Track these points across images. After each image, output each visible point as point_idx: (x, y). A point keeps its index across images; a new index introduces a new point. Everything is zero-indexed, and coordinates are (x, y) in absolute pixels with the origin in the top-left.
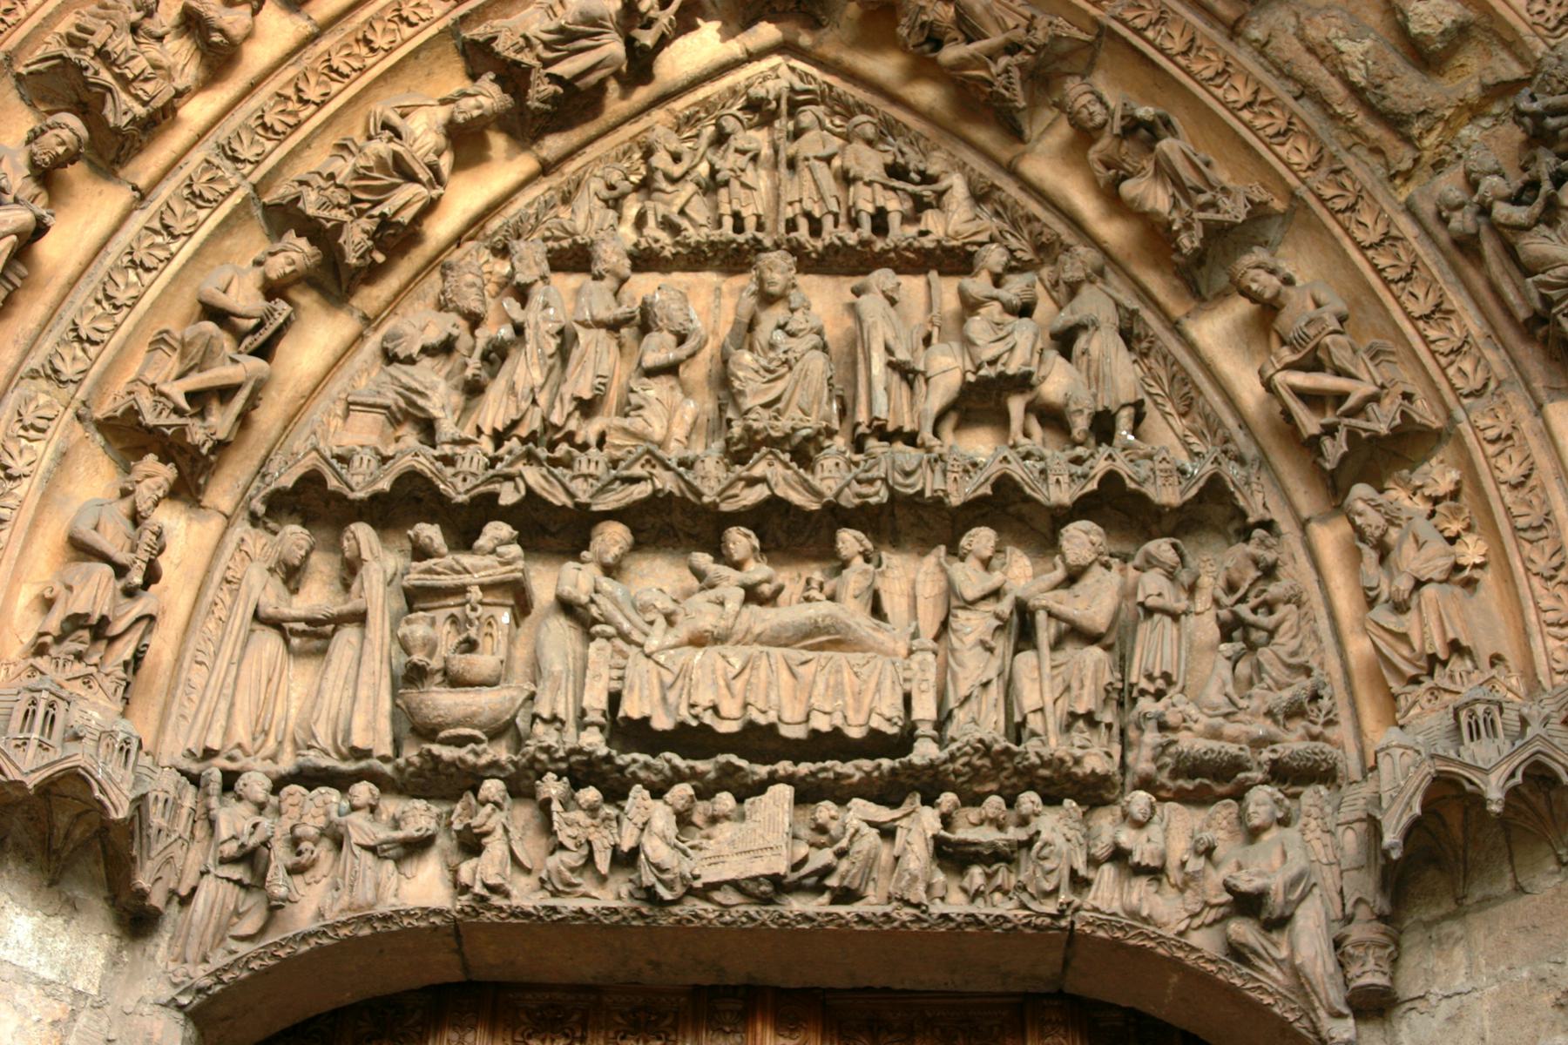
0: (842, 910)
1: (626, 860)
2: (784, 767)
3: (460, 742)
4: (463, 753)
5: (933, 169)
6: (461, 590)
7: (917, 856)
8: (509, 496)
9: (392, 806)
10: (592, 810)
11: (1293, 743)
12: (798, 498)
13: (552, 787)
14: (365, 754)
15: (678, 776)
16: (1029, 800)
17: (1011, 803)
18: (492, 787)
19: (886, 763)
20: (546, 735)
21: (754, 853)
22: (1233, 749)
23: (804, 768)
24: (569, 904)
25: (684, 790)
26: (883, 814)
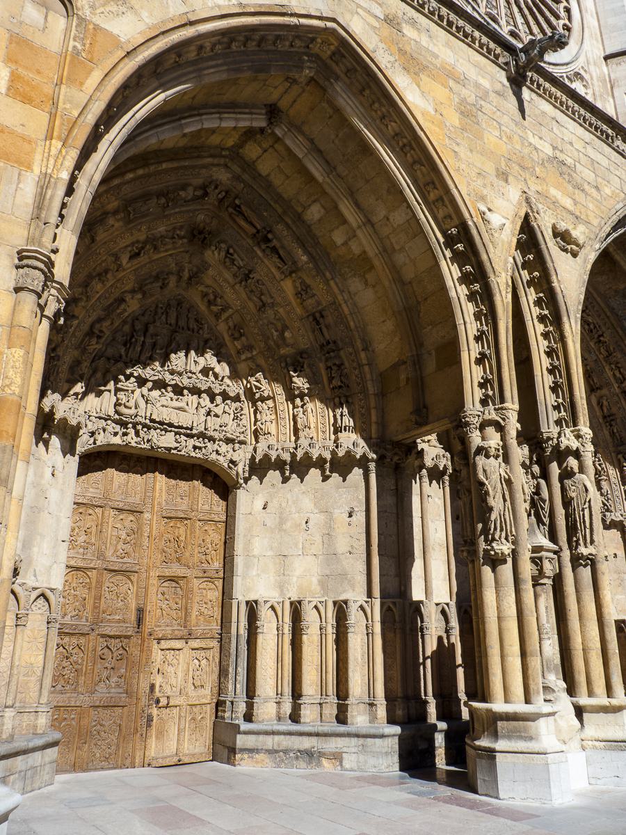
0: (179, 453)
1: (148, 441)
2: (173, 429)
3: (126, 418)
4: (127, 419)
5: (203, 322)
6: (128, 390)
7: (190, 447)
8: (136, 374)
9: (114, 425)
10: (145, 432)
11: (242, 438)
12: (180, 384)
13: (139, 427)
14: (108, 416)
15: (158, 428)
16: (206, 440)
17: (203, 439)
18: (130, 425)
19: (189, 432)
20: (139, 419)
21: (169, 443)
22: (235, 437)
23: (176, 430)
24: (140, 446)
25: (158, 431)
26: (186, 438)
